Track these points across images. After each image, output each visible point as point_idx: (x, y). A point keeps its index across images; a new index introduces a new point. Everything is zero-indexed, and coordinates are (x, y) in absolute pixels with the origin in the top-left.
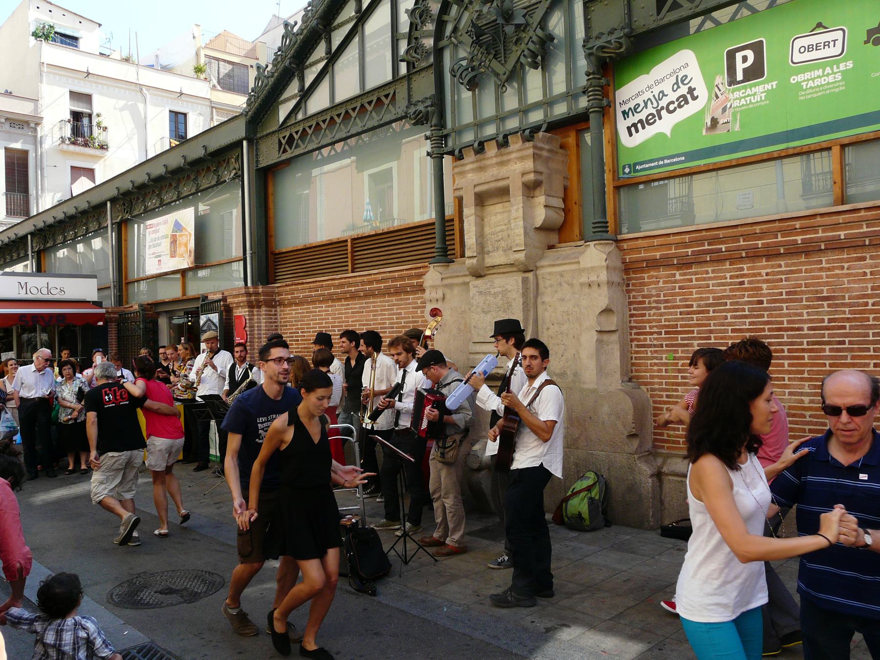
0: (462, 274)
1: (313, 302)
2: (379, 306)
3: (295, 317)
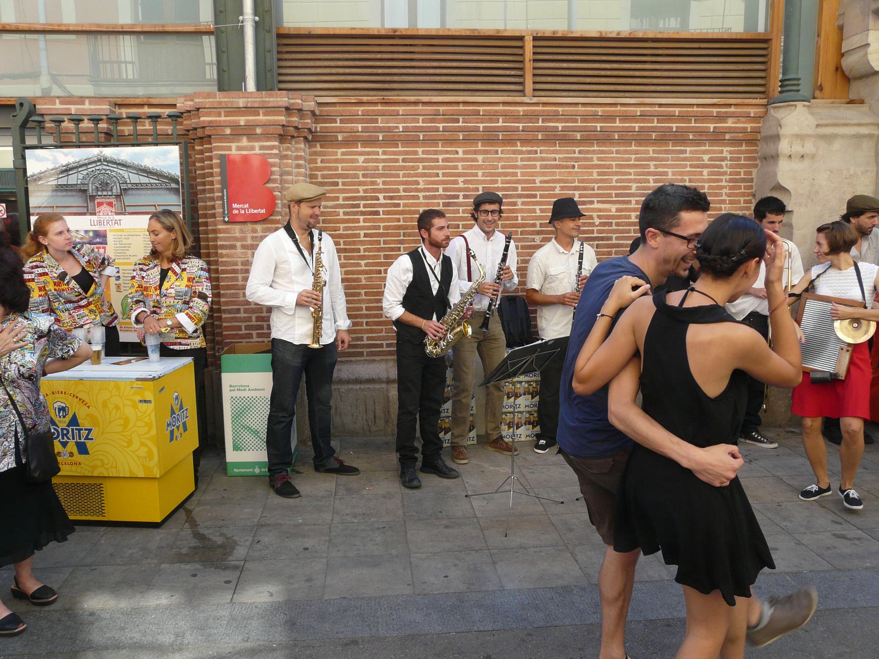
0: (856, 122)
1: (431, 141)
2: (613, 159)
3: (366, 168)
